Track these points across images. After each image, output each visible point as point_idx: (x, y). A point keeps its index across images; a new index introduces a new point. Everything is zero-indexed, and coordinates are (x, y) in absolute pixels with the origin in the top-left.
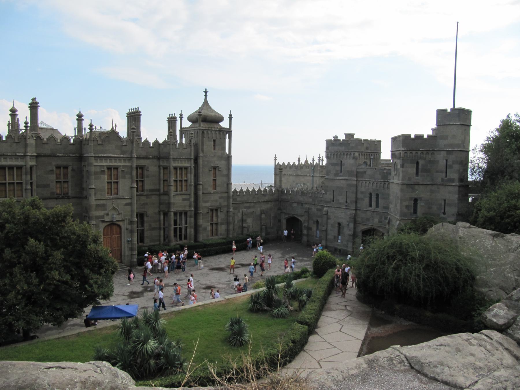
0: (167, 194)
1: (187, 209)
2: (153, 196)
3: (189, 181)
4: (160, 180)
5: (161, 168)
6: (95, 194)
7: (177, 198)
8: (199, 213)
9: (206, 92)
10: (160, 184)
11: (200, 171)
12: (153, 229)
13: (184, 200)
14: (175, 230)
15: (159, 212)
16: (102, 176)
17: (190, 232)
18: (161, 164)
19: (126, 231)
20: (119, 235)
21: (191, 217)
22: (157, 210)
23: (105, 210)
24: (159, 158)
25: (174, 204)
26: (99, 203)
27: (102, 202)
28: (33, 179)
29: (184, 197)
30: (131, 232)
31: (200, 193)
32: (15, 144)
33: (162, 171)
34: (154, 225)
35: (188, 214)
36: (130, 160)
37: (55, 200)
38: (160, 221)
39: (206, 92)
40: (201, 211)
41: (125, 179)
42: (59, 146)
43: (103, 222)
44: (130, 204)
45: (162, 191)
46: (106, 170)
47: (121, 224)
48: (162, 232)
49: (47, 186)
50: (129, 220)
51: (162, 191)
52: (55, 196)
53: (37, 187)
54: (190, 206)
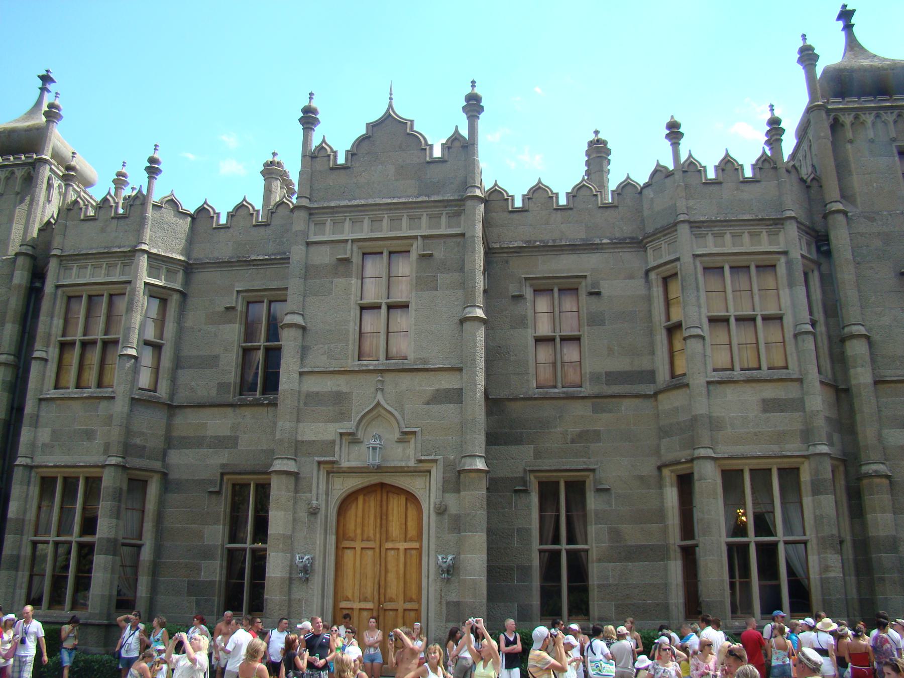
0: (678, 383)
1: (793, 447)
2: (626, 402)
3: (788, 321)
4: (651, 332)
5: (653, 275)
6: (304, 351)
7: (730, 394)
8: (868, 476)
9: (846, 15)
10: (652, 353)
11: (846, 275)
12: (633, 554)
13: (769, 406)
14: (737, 553)
15: (659, 468)
16: (340, 281)
17: (826, 569)
18: (652, 263)
19: (433, 517)
20: (416, 545)
21: (817, 490)
22: (648, 468)
23: (342, 416)
24: (639, 244)
25: (715, 424)
26: (315, 389)
27: (328, 385)
28: (165, 335)
29: (770, 392)
30: (457, 525)
31: (862, 376)
32: (115, 222)
33: (657, 291)
34: (633, 535)
35: (805, 476)
36: (458, 214)
37: (229, 410)
38: (660, 515)
39: (846, 15)
40: (874, 467)
41: (435, 288)
42: (262, 230)
43: (332, 470)
44: (456, 396)
45: (663, 376)
46: (356, 259)
47: (415, 485)
48: (675, 569)
49: (211, 362)
50: (449, 466)
51: (663, 376)
52: (230, 398)
53: (178, 363)
54: (807, 435)
